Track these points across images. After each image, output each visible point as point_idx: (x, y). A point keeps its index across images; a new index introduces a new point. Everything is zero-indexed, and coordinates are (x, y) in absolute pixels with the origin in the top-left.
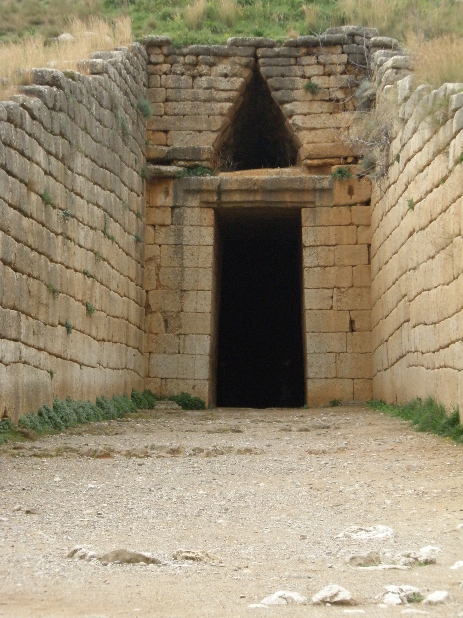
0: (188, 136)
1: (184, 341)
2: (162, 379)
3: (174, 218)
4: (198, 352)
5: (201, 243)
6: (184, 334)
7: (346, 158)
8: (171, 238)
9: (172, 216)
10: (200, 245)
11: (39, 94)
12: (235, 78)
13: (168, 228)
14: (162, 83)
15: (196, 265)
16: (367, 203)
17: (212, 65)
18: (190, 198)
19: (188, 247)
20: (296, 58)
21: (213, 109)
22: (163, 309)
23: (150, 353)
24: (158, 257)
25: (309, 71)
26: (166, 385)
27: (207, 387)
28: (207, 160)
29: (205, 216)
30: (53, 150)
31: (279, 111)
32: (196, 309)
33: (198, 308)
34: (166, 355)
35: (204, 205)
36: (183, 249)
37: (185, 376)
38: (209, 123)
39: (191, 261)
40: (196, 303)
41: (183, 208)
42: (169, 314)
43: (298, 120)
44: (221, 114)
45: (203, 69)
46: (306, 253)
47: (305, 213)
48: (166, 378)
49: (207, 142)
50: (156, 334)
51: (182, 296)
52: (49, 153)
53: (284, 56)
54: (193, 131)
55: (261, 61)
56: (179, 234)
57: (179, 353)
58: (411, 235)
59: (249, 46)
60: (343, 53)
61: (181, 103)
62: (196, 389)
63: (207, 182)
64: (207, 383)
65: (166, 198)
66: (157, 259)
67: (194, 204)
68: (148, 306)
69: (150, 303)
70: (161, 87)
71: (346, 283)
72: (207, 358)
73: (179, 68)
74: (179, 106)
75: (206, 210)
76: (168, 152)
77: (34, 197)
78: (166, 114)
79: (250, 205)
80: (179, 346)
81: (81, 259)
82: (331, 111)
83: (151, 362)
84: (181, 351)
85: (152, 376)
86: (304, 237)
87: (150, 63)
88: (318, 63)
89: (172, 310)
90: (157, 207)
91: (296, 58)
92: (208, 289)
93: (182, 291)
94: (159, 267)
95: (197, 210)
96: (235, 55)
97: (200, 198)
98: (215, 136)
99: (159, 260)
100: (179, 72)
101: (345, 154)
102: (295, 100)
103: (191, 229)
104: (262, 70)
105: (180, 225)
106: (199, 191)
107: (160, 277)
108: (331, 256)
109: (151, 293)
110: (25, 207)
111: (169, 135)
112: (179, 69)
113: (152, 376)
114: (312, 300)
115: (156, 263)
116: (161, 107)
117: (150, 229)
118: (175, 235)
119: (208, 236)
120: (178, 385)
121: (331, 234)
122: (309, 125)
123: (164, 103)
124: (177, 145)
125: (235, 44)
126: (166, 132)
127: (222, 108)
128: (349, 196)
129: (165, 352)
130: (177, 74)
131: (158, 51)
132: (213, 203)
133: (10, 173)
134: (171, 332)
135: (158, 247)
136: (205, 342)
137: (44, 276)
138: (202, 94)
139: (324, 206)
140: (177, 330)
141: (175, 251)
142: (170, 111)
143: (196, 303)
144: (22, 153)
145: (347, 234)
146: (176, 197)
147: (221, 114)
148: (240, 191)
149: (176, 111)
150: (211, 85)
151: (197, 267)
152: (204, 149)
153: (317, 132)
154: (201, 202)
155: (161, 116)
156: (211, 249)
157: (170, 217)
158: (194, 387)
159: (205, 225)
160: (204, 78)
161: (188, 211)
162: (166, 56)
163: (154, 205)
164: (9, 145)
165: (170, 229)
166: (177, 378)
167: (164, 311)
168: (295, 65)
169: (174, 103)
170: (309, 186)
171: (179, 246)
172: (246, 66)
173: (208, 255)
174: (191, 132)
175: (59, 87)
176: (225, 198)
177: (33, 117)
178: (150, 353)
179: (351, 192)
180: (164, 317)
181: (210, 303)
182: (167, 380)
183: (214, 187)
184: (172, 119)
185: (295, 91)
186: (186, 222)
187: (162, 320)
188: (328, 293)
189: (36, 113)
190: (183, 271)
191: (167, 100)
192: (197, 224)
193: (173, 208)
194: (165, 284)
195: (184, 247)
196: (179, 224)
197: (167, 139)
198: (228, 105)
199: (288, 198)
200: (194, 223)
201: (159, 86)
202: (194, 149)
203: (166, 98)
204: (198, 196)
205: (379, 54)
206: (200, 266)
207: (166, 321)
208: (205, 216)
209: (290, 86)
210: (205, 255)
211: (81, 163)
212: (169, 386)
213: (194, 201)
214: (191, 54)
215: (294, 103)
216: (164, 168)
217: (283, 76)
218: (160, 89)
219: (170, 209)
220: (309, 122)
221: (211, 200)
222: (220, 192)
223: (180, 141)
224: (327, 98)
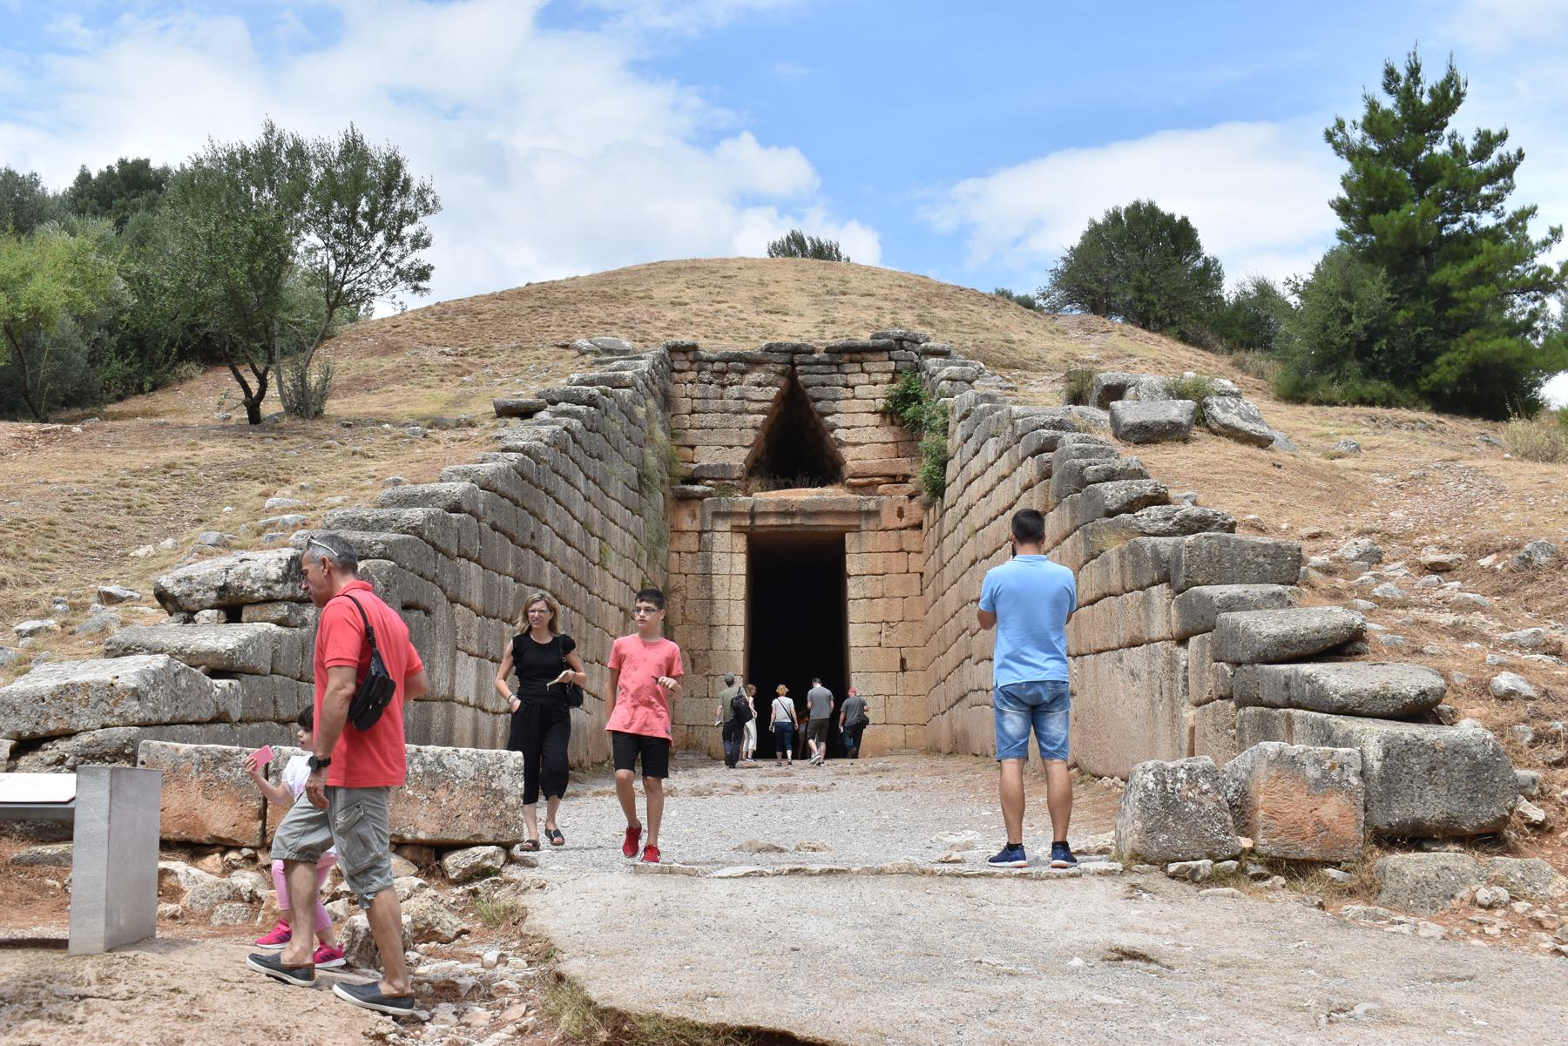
11: (577, 415)
17: (743, 373)
18: (719, 522)
20: (838, 365)
25: (852, 379)
28: (739, 478)
30: (591, 473)
31: (818, 425)
38: (741, 438)
43: (840, 434)
44: (754, 427)
46: (850, 582)
47: (849, 538)
49: (738, 458)
52: (588, 477)
53: (823, 363)
56: (707, 563)
58: (973, 563)
59: (786, 352)
71: (896, 617)
77: (576, 525)
81: (614, 590)
86: (848, 565)
91: (838, 365)
94: (685, 599)
96: (769, 362)
98: (747, 451)
101: (893, 472)
104: (800, 378)
108: (879, 586)
110: (569, 536)
112: (706, 376)
114: (858, 635)
117: (675, 555)
119: (740, 564)
121: (878, 562)
122: (853, 440)
126: (693, 447)
131: (683, 357)
133: (557, 501)
137: (584, 610)
138: (733, 405)
142: (697, 424)
144: (566, 479)
145: (898, 562)
146: (703, 521)
147: (754, 427)
148: (777, 514)
156: (743, 579)
162: (692, 362)
164: (556, 472)
170: (853, 507)
171: (707, 576)
172: (782, 374)
175: (596, 407)
176: (759, 522)
177: (575, 441)
188: (877, 628)
189: (579, 436)
191: (694, 412)
193: (700, 533)
198: (763, 417)
199: (829, 522)
205: (931, 362)
207: (693, 660)
211: (617, 488)
213: (723, 525)
216: (689, 487)
220: (852, 436)
222: (753, 515)
223: (707, 457)
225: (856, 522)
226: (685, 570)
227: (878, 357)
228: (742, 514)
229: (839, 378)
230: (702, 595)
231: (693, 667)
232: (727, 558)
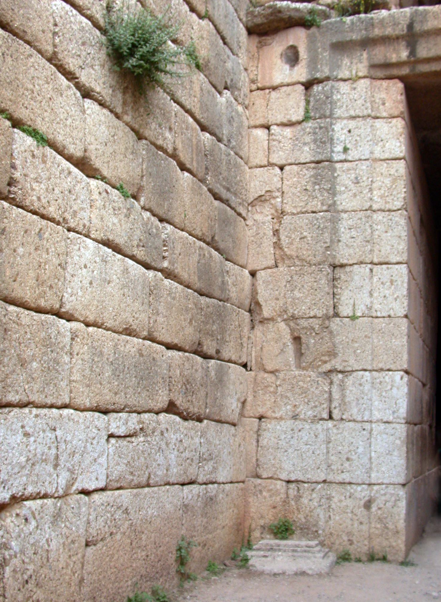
1: (342, 387)
2: (288, 482)
3: (312, 104)
4: (377, 415)
5: (377, 155)
6: (341, 372)
8: (306, 148)
9: (308, 102)
10: (376, 160)
13: (299, 127)
15: (367, 205)
18: (346, 61)
19: (346, 165)
22: (291, 311)
23: (260, 418)
24: (278, 194)
26: (298, 498)
27: (403, 504)
29: (383, 95)
32: (370, 309)
33: (377, 306)
34: (298, 424)
35: (380, 73)
36: (335, 170)
37: (346, 477)
39: (355, 195)
40: (371, 295)
41: (330, 83)
42: (304, 323)
48: (297, 481)
50: (272, 372)
51: (334, 279)
56: (324, 139)
57: (331, 418)
62: (374, 508)
63: (382, 21)
64: (402, 493)
66: (274, 198)
68: (254, 307)
69: (261, 300)
72: (401, 430)
75: (385, 83)
80: (330, 400)
83: (264, 442)
84: (336, 414)
85: (265, 475)
89: (312, 314)
92: (398, 259)
93: (335, 267)
95: (364, 84)
97: (369, 59)
99: (279, 200)
103: (352, 124)
105: (325, 117)
106: (367, 43)
107: (283, 237)
109: (261, 275)
113: (265, 475)
115: (274, 206)
117: (261, 133)
118: (315, 141)
119: (392, 139)
120: (329, 498)
129: (295, 417)
132: (399, 64)
134: (311, 366)
135: (277, 170)
136: (395, 390)
140: (325, 362)
141: (315, 176)
143: (371, 295)
146: (313, 62)
151: (370, 208)
154: (373, 66)
156: (401, 168)
157: (303, 104)
158: (368, 505)
159: (385, 114)
161: (344, 87)
163: (268, 84)
165: (304, 130)
166: (324, 481)
167: (293, 318)
173: (394, 181)
178: (260, 418)
180: (292, 330)
181: (405, 293)
182: (301, 485)
183: (402, 29)
186: (338, 112)
187: (287, 338)
190: (335, 221)
192: (365, 113)
193: (308, 85)
194: (294, 254)
195: (338, 165)
196: (323, 116)
200: (358, 112)
204: (365, 55)
206: (375, 207)
207: (297, 340)
208: (383, 95)
210: (388, 181)
212: (305, 501)
221: (394, 58)
226: (275, 159)
228: (385, 40)
230: (316, 204)
231: (299, 354)
232: (363, 128)
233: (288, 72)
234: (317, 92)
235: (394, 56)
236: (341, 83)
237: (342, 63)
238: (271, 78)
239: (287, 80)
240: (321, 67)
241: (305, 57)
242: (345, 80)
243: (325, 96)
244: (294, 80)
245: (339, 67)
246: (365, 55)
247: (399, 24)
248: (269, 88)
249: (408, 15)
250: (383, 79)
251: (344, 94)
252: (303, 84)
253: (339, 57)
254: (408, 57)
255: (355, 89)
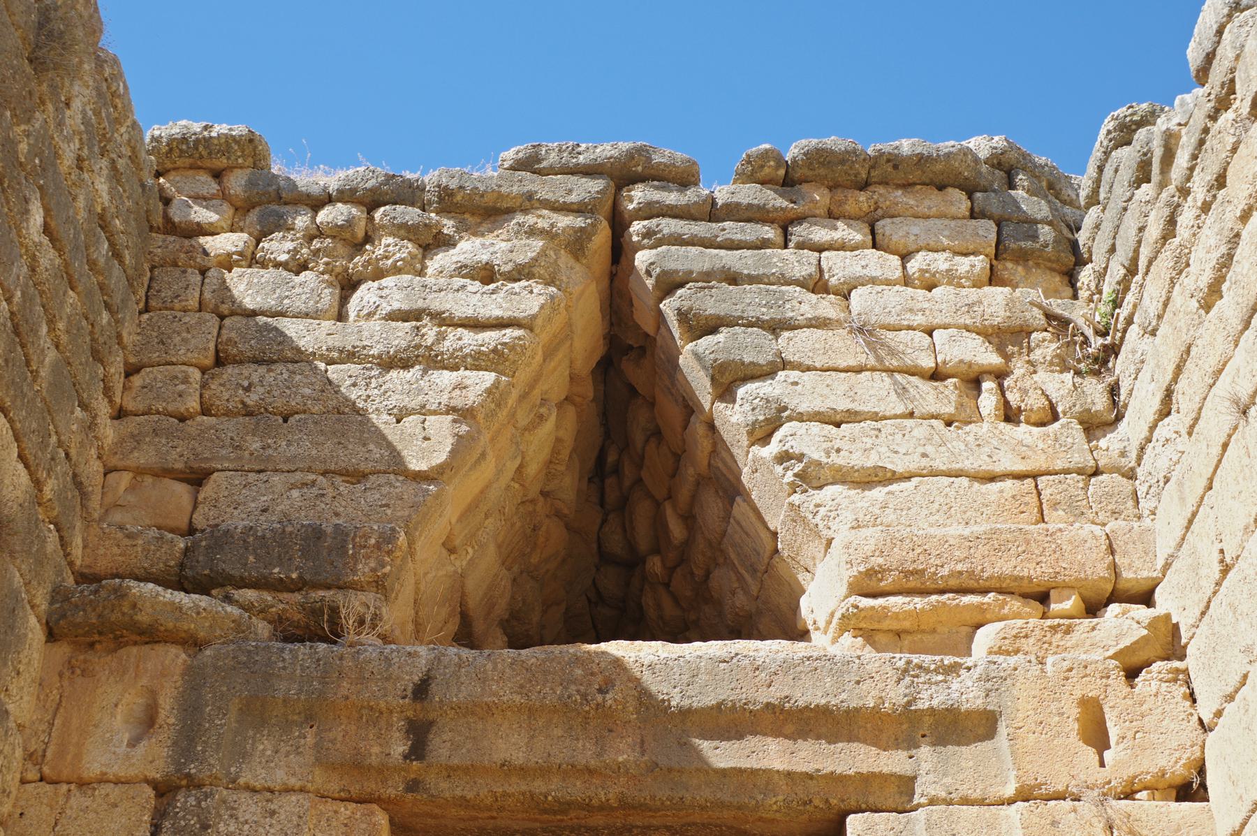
0: (295, 493)
7: (1043, 598)
12: (523, 283)
14: (207, 295)
16: (1190, 789)
18: (265, 746)
21: (420, 390)
25: (838, 266)
43: (806, 439)
45: (390, 247)
54: (324, 474)
55: (637, 227)
59: (589, 171)
60: (973, 215)
61: (279, 367)
65: (133, 743)
67: (280, 777)
70: (200, 310)
73: (289, 245)
74: (270, 378)
75: (346, 810)
76: (187, 550)
78: (205, 411)
79: (576, 790)
82: (949, 409)
87: (171, 227)
88: (874, 246)
90: (83, 784)
96: (529, 203)
97: (317, 746)
100: (284, 257)
102: (785, 365)
111: (207, 491)
116: (186, 381)
122: (855, 458)
123: (204, 371)
124: (237, 521)
125: (528, 164)
126: (196, 478)
127: (460, 386)
128: (1091, 754)
130: (277, 265)
132: (382, 771)
139: (966, 801)
146: (189, 738)
149: (252, 399)
150: (420, 304)
152: (366, 537)
153: (894, 487)
155: (182, 419)
160: (388, 281)
161: (249, 807)
162: (242, 208)
163: (66, 773)
168: (786, 247)
169: (247, 370)
174: (311, 477)
179: (1096, 736)
184: (230, 427)
185: (786, 334)
193: (164, 790)
197: (195, 505)
199: (771, 755)
201: (193, 303)
202: (317, 534)
203: (217, 351)
209: (767, 315)
214: (346, 195)
215: (781, 375)
217: (733, 279)
218: (191, 319)
219: (149, 792)
220: (856, 448)
224: (927, 363)
225: (893, 762)
227: (931, 201)
229: (797, 263)
233: (123, 749)
234: (184, 808)
235: (376, 750)
236: (244, 796)
237: (254, 748)
238: (78, 757)
239: (117, 770)
240: (204, 751)
241: (172, 720)
242: (254, 791)
243: (199, 821)
244: (132, 772)
245: (244, 756)
246: (310, 740)
247: (398, 678)
248: (69, 783)
249: (422, 663)
250: (342, 800)
251: (246, 822)
252: (154, 784)
253: (251, 733)
254: (406, 757)
255: (273, 813)
